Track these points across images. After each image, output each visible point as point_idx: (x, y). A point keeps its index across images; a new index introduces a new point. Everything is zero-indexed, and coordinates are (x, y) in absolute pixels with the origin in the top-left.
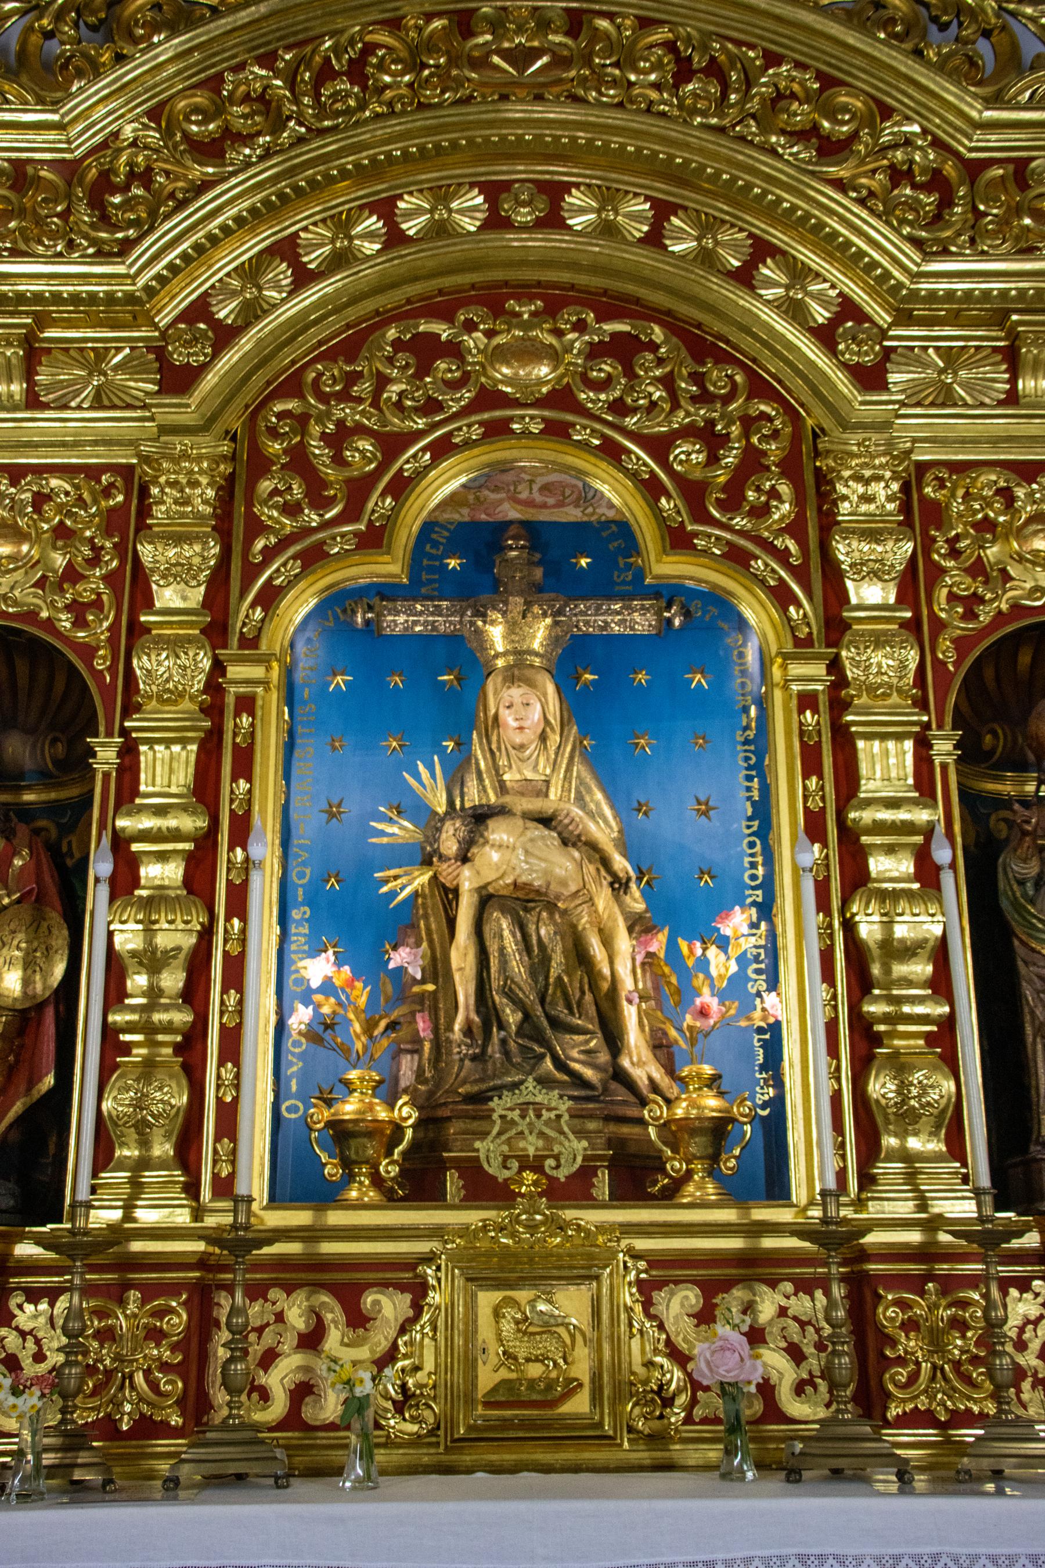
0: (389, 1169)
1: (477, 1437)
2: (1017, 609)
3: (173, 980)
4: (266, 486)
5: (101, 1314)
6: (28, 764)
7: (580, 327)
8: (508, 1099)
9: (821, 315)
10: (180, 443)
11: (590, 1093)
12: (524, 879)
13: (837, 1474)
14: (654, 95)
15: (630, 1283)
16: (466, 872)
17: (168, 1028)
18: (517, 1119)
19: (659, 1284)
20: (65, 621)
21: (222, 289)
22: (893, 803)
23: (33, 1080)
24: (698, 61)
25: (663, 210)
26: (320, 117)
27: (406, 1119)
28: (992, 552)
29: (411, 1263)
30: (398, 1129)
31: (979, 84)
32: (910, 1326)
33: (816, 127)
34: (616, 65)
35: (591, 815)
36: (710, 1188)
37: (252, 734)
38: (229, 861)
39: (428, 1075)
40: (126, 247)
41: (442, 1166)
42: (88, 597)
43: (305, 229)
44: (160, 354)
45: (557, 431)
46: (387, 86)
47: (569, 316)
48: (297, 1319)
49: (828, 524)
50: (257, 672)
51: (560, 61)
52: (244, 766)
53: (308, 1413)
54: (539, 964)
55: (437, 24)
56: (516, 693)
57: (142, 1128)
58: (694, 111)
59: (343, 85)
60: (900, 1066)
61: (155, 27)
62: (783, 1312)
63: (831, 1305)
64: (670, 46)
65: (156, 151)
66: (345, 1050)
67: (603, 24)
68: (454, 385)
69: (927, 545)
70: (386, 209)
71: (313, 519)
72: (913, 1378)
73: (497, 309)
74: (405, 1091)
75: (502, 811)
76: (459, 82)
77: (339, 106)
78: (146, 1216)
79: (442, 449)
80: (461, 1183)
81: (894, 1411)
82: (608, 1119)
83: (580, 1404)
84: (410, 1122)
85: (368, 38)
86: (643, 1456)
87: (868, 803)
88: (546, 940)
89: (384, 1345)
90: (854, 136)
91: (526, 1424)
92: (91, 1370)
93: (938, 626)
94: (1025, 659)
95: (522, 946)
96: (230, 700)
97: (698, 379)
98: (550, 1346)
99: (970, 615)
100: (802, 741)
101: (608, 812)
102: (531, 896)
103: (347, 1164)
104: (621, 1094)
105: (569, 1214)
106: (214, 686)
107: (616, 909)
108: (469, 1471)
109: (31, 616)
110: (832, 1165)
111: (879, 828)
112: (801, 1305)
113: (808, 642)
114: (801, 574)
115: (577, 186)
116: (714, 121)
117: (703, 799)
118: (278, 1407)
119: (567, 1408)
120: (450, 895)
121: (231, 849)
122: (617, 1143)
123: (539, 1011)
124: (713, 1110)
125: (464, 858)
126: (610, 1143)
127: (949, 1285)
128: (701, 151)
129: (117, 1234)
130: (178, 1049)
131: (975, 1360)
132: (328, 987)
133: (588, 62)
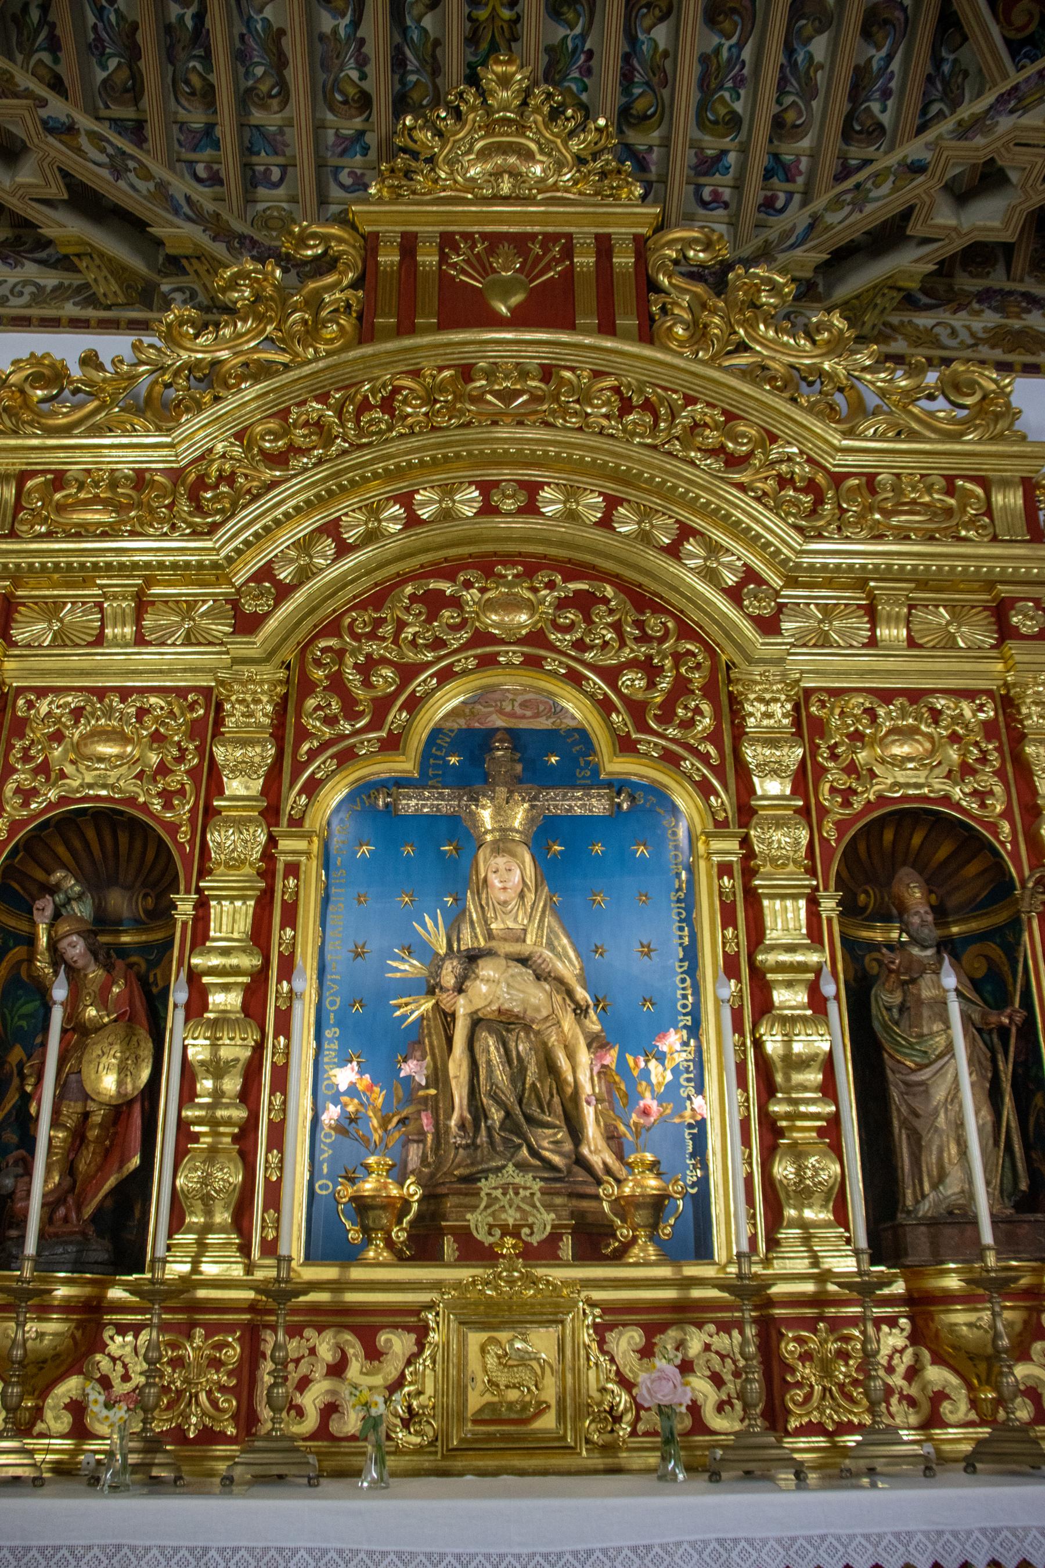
0: (399, 1235)
1: (467, 1448)
2: (881, 799)
3: (232, 1084)
4: (311, 703)
5: (174, 1346)
6: (126, 914)
7: (551, 585)
8: (493, 1180)
9: (730, 579)
10: (247, 671)
11: (557, 1175)
12: (506, 1006)
13: (748, 1473)
14: (605, 422)
15: (588, 1327)
16: (461, 1000)
17: (228, 1122)
18: (500, 1196)
19: (611, 1327)
20: (157, 805)
22: (791, 949)
23: (124, 1161)
24: (636, 400)
25: (612, 503)
26: (359, 436)
27: (412, 1196)
28: (862, 756)
29: (416, 1310)
30: (406, 1203)
31: (837, 422)
32: (806, 1357)
33: (723, 448)
34: (577, 401)
35: (559, 956)
36: (651, 1250)
37: (297, 893)
38: (277, 991)
39: (430, 1160)
40: (214, 528)
41: (441, 1232)
42: (174, 786)
43: (346, 514)
44: (235, 604)
45: (533, 663)
46: (409, 415)
47: (542, 577)
48: (326, 1353)
49: (739, 734)
50: (301, 845)
51: (536, 399)
52: (290, 917)
53: (334, 1427)
54: (518, 1073)
55: (447, 373)
56: (501, 861)
57: (207, 1200)
58: (634, 434)
59: (377, 414)
60: (798, 1154)
61: (243, 378)
62: (707, 1347)
63: (744, 1343)
64: (616, 390)
65: (239, 461)
66: (366, 1141)
67: (567, 374)
68: (455, 628)
69: (814, 750)
70: (406, 500)
71: (346, 727)
72: (808, 1398)
73: (488, 572)
74: (412, 1172)
75: (490, 953)
76: (462, 413)
77: (373, 428)
78: (209, 1269)
79: (445, 676)
80: (456, 1246)
81: (793, 1424)
82: (571, 1195)
83: (548, 1422)
84: (416, 1197)
85: (396, 383)
86: (598, 1462)
87: (772, 948)
88: (523, 1054)
89: (394, 1375)
90: (751, 454)
91: (506, 1437)
92: (165, 1390)
93: (823, 812)
94: (888, 836)
95: (504, 1059)
96: (280, 867)
97: (639, 624)
98: (524, 1375)
99: (847, 804)
100: (721, 900)
101: (572, 954)
102: (512, 1020)
103: (366, 1230)
104: (581, 1176)
105: (539, 1272)
106: (268, 855)
107: (578, 1030)
108: (461, 1474)
109: (132, 801)
110: (746, 1231)
111: (781, 967)
112: (722, 1342)
113: (725, 824)
114: (719, 772)
115: (549, 484)
116: (649, 441)
117: (645, 942)
118: (311, 1422)
119: (539, 1424)
120: (448, 1018)
121: (279, 982)
122: (578, 1215)
123: (517, 1110)
124: (653, 1189)
125: (460, 990)
126: (573, 1215)
127: (836, 1324)
128: (640, 461)
129: (187, 1283)
130: (236, 1139)
131: (855, 1383)
132: (352, 1090)
133: (557, 400)
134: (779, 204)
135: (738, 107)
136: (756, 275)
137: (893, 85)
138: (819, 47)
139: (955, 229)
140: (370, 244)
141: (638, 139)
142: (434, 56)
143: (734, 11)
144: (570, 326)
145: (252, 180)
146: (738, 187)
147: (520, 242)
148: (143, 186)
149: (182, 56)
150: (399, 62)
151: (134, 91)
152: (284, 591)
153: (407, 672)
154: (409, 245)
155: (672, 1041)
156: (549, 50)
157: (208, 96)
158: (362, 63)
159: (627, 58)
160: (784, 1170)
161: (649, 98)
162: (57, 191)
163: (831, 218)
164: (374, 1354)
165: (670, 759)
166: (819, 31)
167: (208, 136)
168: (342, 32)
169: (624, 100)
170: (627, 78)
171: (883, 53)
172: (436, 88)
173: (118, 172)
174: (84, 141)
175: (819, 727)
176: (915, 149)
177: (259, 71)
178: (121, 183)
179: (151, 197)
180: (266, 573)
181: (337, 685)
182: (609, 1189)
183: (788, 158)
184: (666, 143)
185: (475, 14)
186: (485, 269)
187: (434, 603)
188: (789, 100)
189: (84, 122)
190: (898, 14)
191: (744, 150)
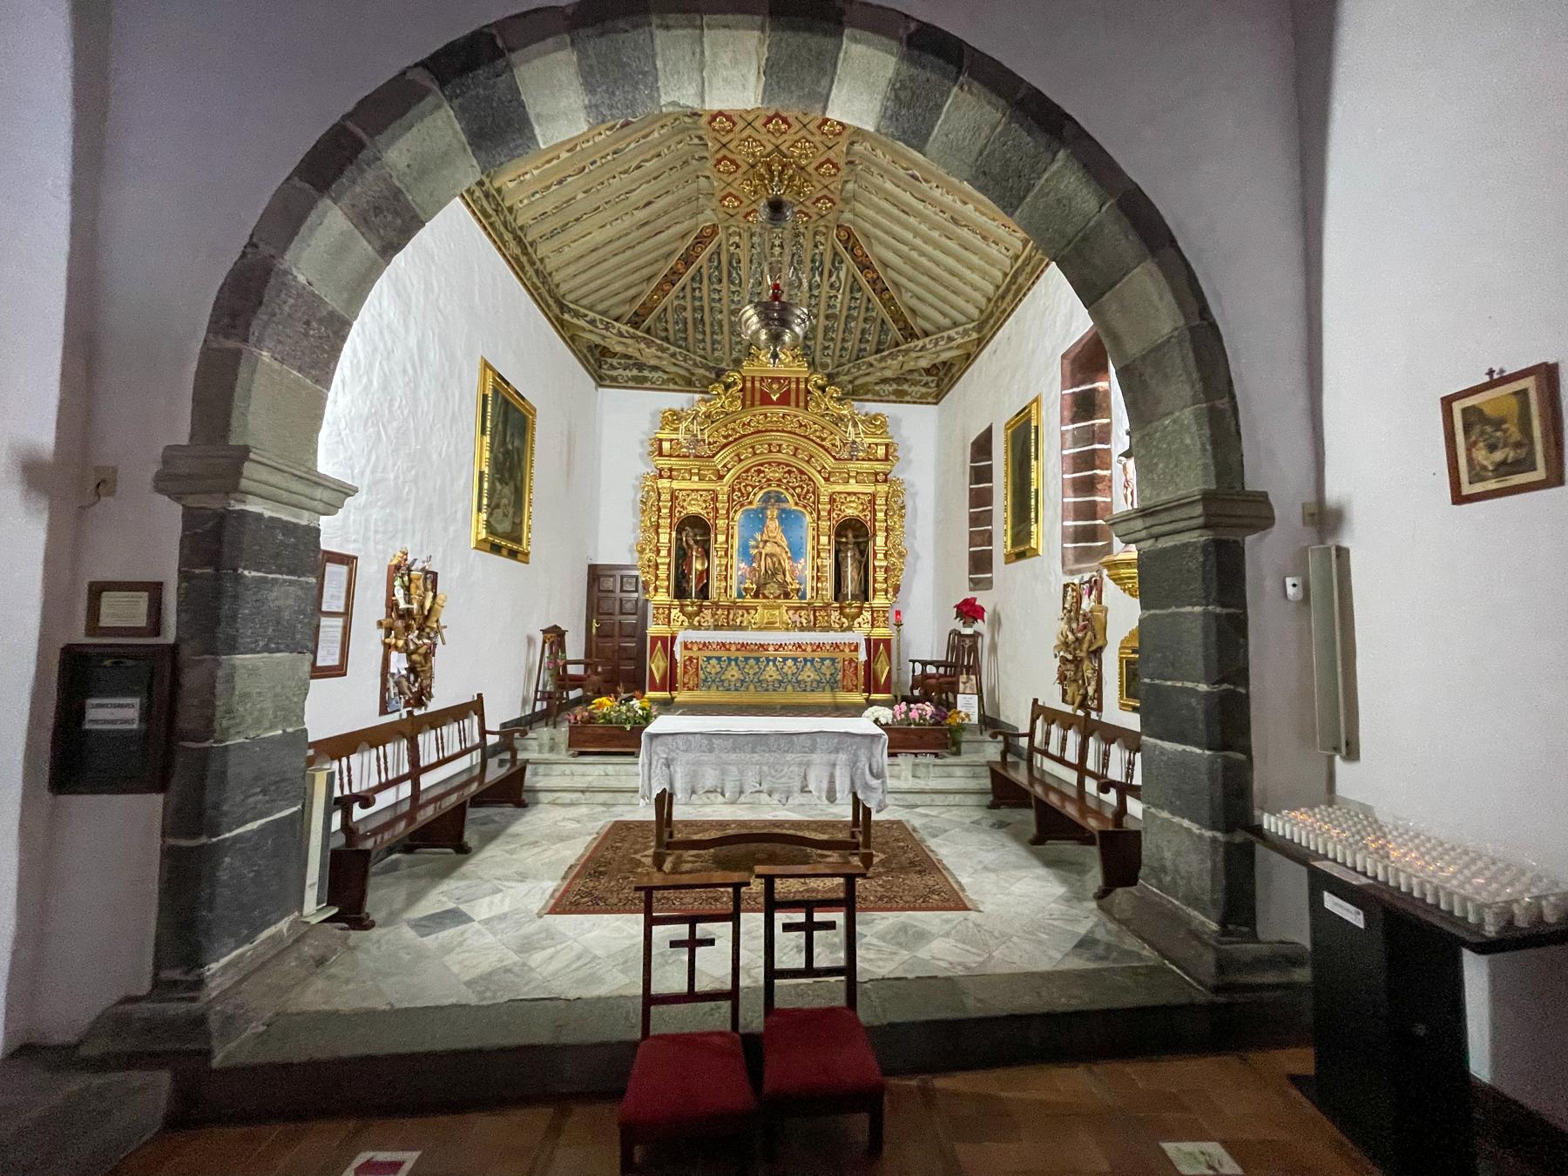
3: (724, 568)
9: (819, 469)
21: (729, 462)
25: (796, 449)
28: (843, 507)
45: (779, 486)
48: (740, 613)
52: (732, 537)
54: (774, 564)
60: (822, 582)
79: (761, 488)
83: (777, 625)
120: (761, 553)
138: (852, 324)
140: (744, 379)
144: (789, 404)
145: (713, 350)
148: (691, 362)
151: (686, 330)
152: (729, 470)
153: (754, 487)
155: (802, 561)
157: (704, 333)
160: (819, 585)
163: (853, 370)
164: (748, 613)
165: (805, 507)
167: (703, 341)
173: (685, 361)
174: (678, 356)
175: (835, 500)
176: (871, 359)
180: (725, 466)
181: (740, 490)
182: (790, 587)
186: (771, 388)
187: (759, 472)
191: (835, 344)
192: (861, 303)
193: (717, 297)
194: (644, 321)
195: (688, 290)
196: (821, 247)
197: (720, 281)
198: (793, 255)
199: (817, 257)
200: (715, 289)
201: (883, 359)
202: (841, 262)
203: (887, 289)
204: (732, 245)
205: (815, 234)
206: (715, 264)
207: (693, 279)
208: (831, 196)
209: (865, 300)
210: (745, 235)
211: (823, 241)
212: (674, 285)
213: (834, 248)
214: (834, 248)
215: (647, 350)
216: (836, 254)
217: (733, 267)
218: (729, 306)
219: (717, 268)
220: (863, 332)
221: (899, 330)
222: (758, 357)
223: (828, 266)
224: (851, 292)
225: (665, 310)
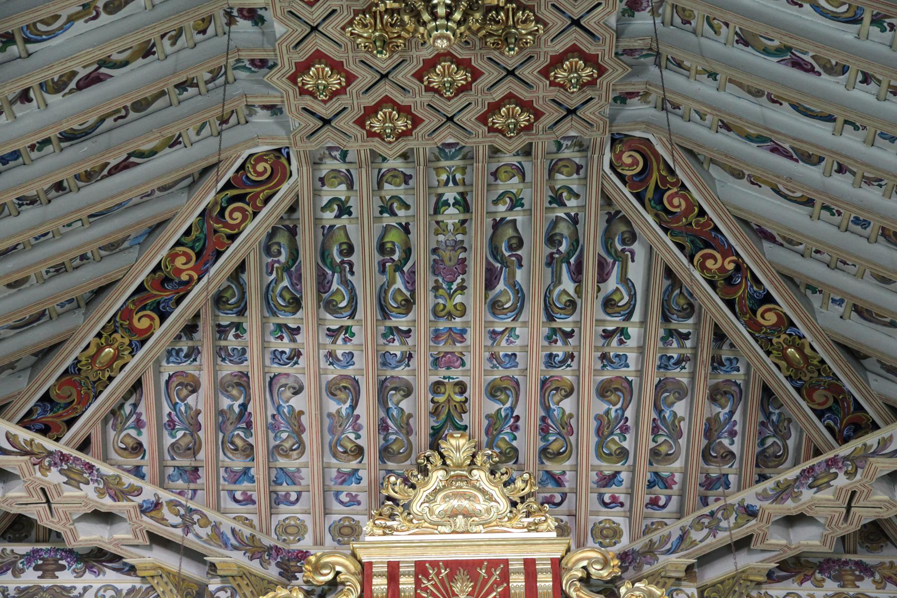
134: (661, 503)
135: (625, 444)
136: (638, 589)
137: (737, 428)
138: (680, 408)
139: (786, 546)
140: (365, 571)
141: (554, 467)
142: (408, 424)
143: (617, 389)
146: (631, 494)
147: (470, 567)
148: (204, 532)
149: (231, 428)
150: (383, 427)
151: (193, 450)
154: (393, 572)
156: (488, 417)
158: (357, 429)
159: (543, 419)
161: (561, 441)
162: (144, 540)
163: (696, 535)
166: (679, 399)
168: (344, 412)
169: (542, 444)
170: (544, 431)
171: (727, 410)
172: (410, 443)
173: (187, 528)
176: (749, 496)
177: (284, 435)
178: (191, 536)
179: (209, 540)
183: (665, 474)
184: (575, 469)
185: (436, 399)
188: (661, 440)
189: (165, 496)
190: (734, 388)
192: (695, 348)
193: (285, 346)
194: (70, 423)
195: (205, 336)
196: (572, 203)
197: (296, 304)
198: (497, 225)
199: (563, 229)
200: (280, 327)
201: (783, 492)
202: (633, 237)
203: (768, 298)
204: (328, 207)
205: (552, 170)
206: (283, 258)
207: (219, 300)
208: (590, 48)
209: (707, 335)
210: (364, 179)
211: (575, 187)
212: (163, 317)
213: (607, 200)
214: (607, 200)
215: (70, 492)
216: (614, 217)
217: (333, 266)
218: (320, 373)
219: (286, 269)
220: (711, 429)
221: (820, 414)
222: (407, 507)
223: (593, 248)
224: (666, 319)
225: (137, 386)
